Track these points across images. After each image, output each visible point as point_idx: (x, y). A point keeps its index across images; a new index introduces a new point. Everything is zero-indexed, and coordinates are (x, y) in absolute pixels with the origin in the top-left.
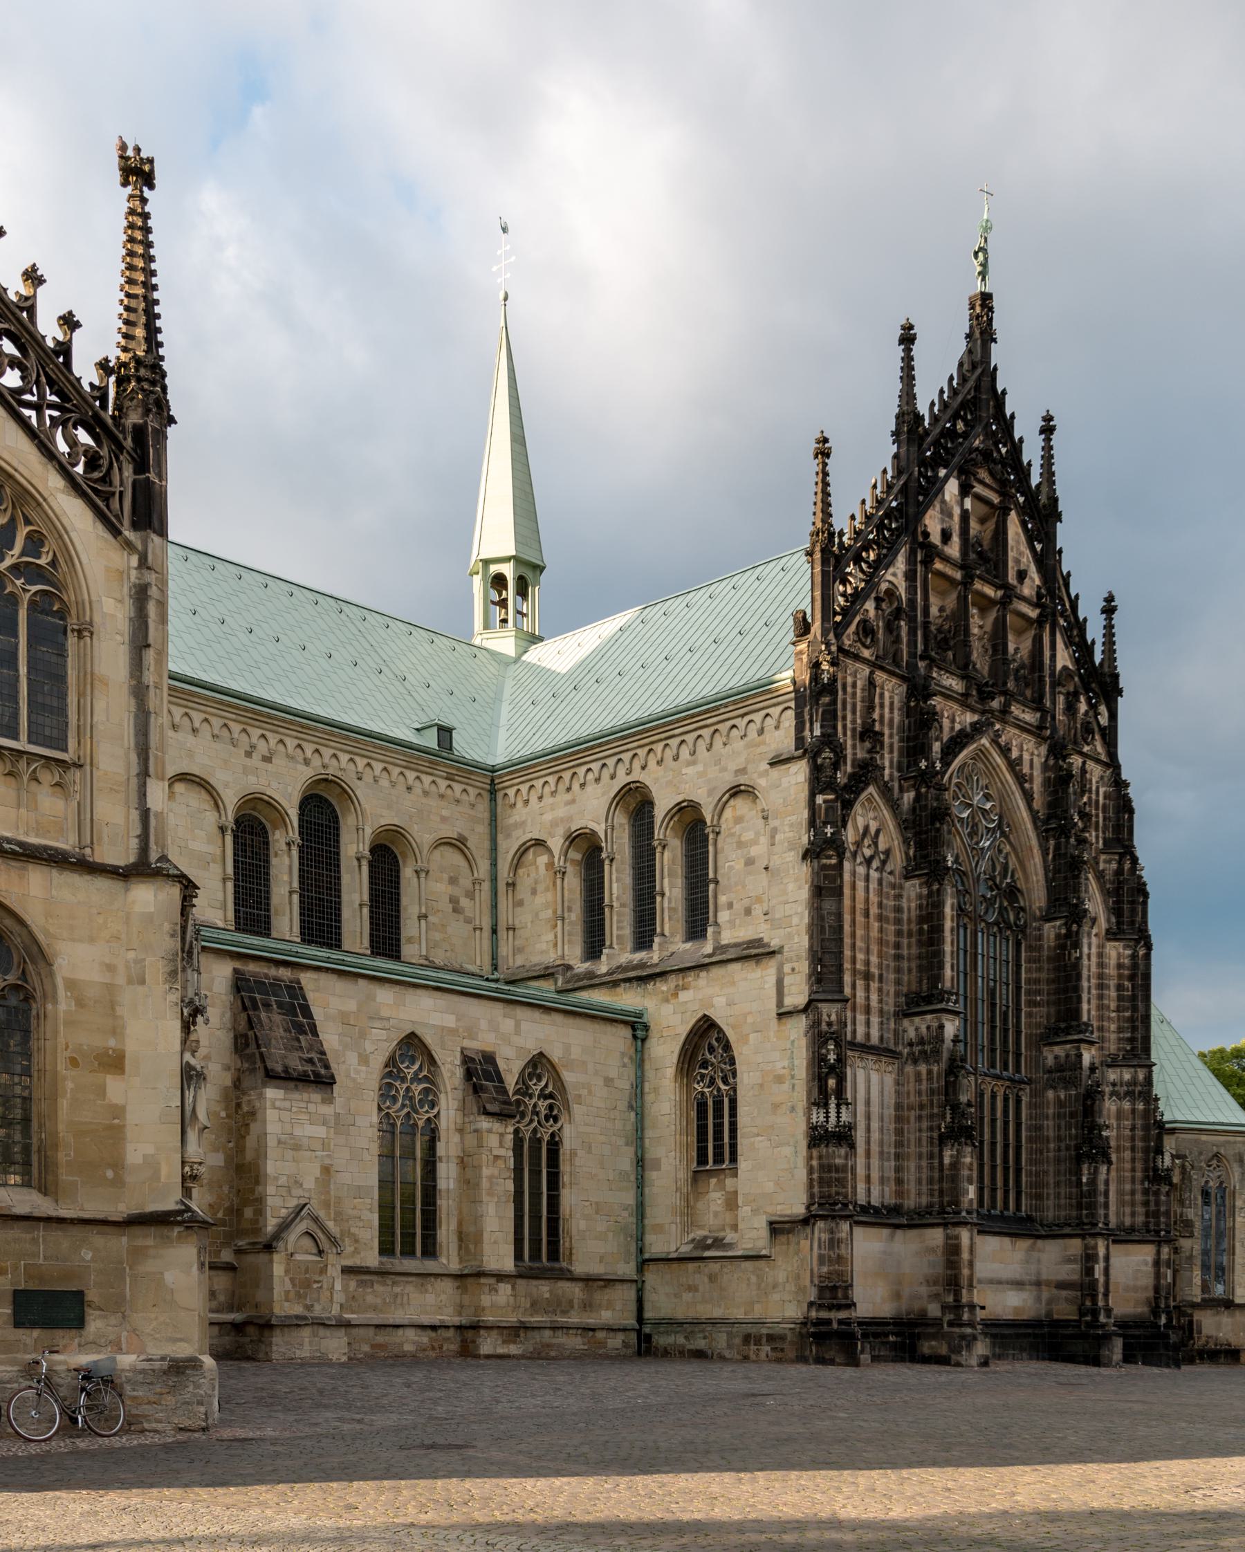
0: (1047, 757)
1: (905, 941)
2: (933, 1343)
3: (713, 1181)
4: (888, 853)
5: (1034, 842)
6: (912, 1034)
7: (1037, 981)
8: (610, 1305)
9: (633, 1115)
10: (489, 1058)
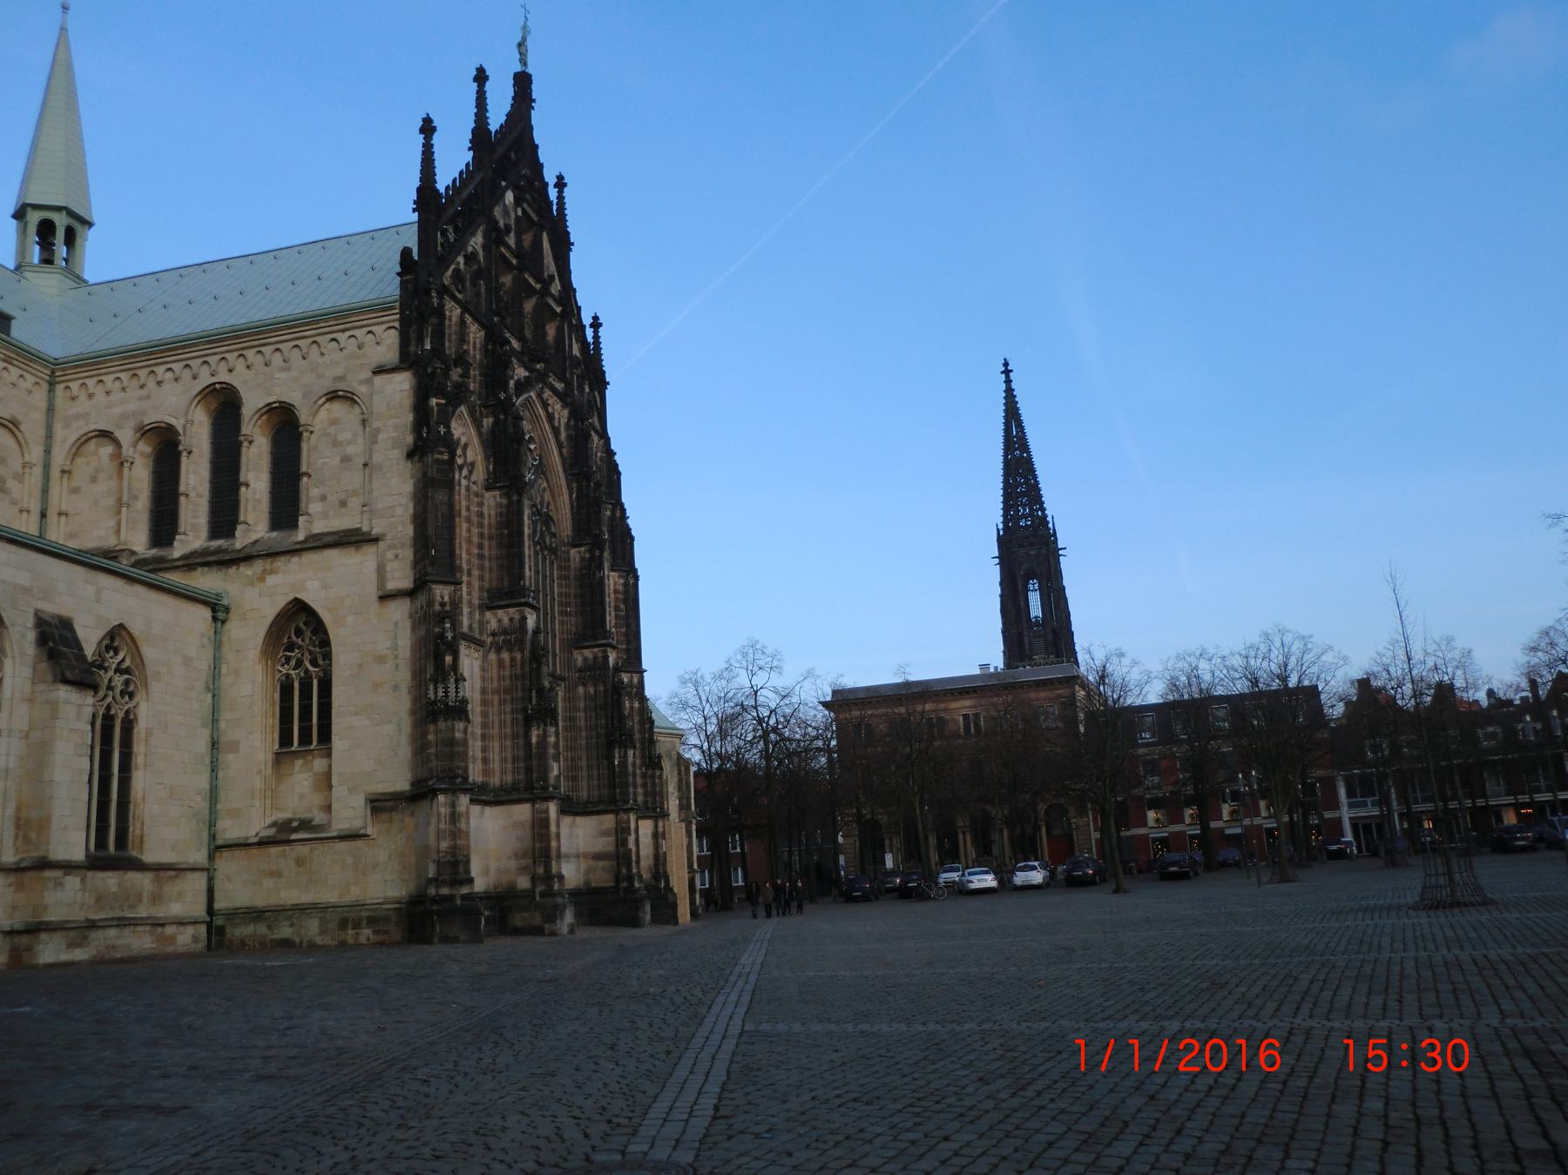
0: (569, 419)
1: (486, 543)
2: (525, 915)
3: (299, 763)
4: (472, 465)
5: (563, 482)
6: (493, 625)
7: (567, 595)
8: (180, 897)
9: (209, 696)
10: (66, 624)
